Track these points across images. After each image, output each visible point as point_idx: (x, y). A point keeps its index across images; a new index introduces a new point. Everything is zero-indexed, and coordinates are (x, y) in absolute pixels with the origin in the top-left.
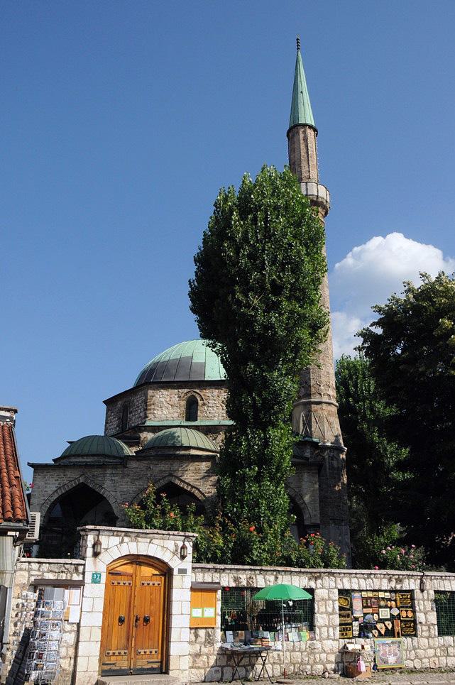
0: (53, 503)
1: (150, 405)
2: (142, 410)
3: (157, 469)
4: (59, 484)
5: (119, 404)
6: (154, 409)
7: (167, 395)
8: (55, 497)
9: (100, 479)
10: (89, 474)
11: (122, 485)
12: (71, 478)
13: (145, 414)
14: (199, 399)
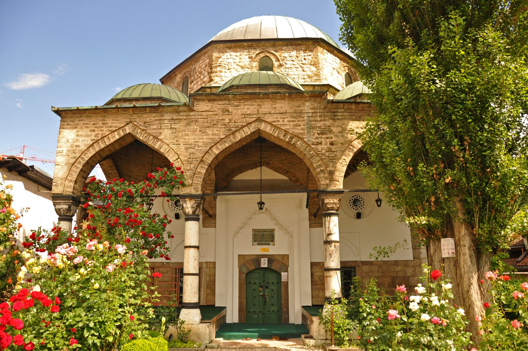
0: (87, 163)
1: (216, 67)
2: (206, 74)
3: (239, 112)
4: (96, 135)
5: (178, 78)
6: (221, 71)
7: (236, 56)
8: (92, 153)
9: (155, 127)
10: (139, 120)
11: (187, 135)
12: (113, 130)
13: (210, 77)
14: (274, 60)
